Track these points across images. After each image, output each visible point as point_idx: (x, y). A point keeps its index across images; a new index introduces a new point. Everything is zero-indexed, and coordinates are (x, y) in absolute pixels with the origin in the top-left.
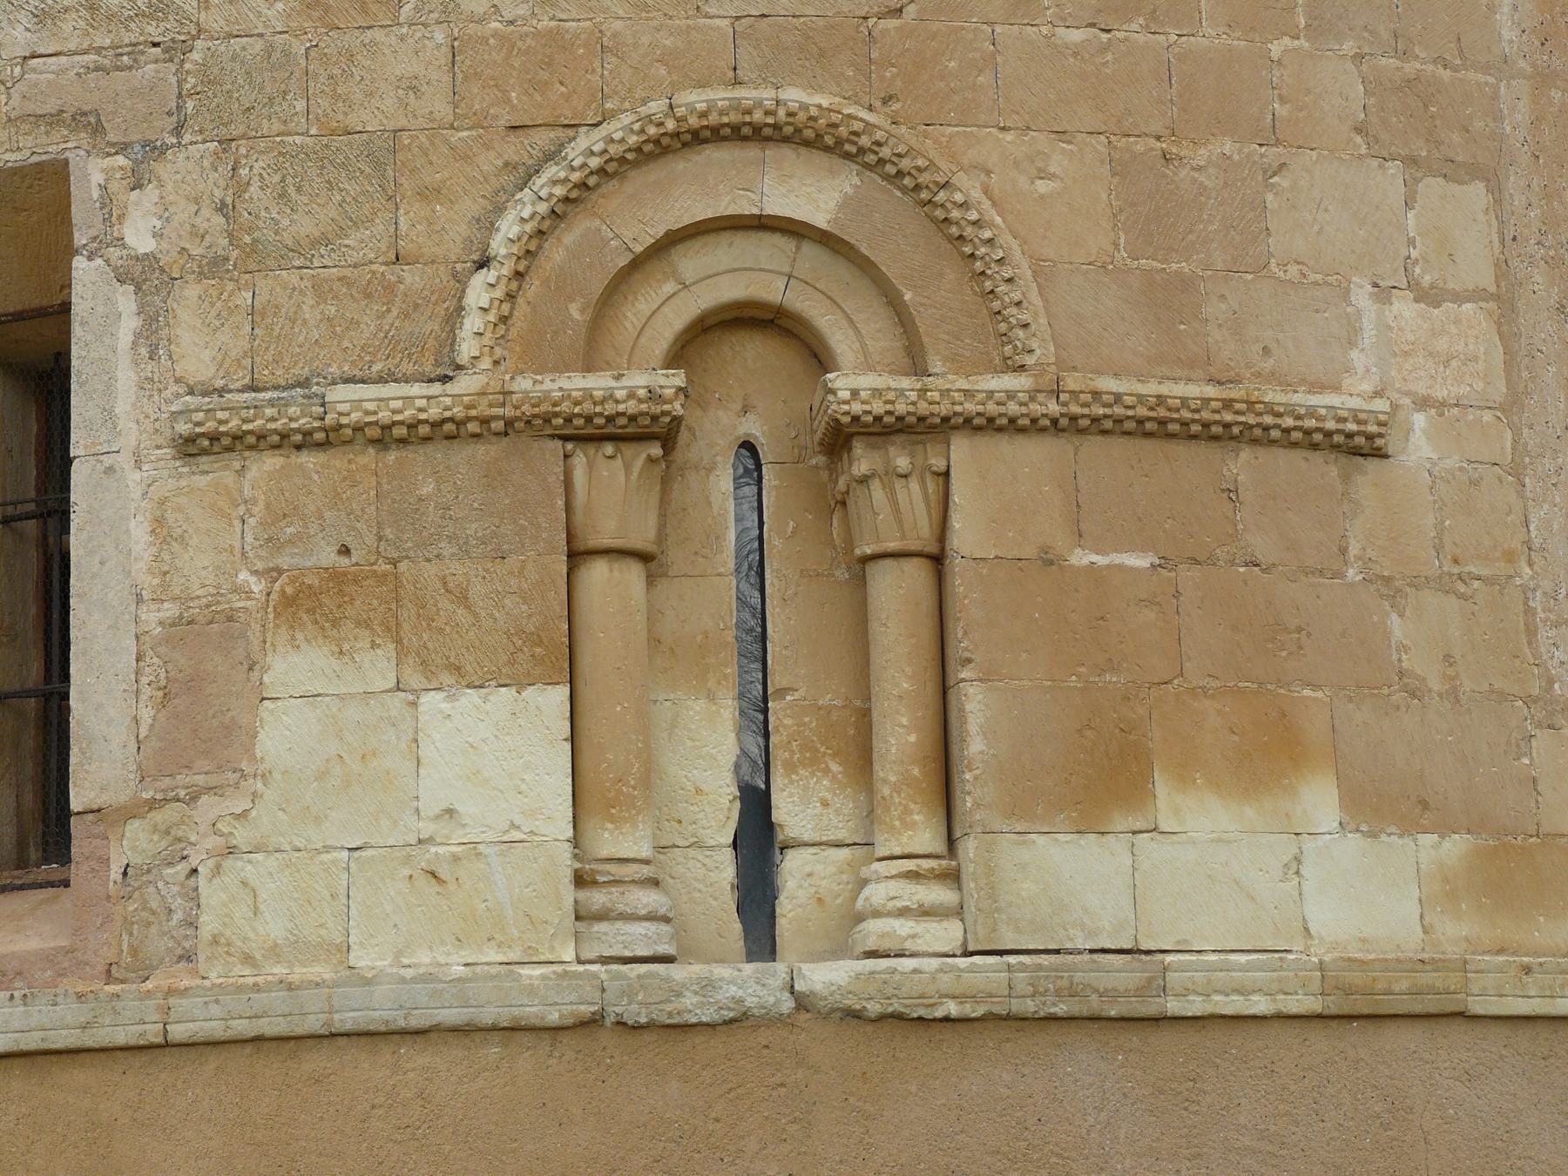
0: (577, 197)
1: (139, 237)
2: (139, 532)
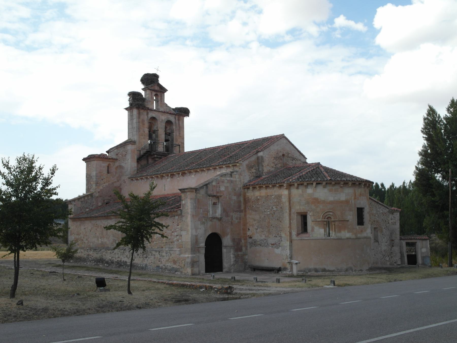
0: (324, 214)
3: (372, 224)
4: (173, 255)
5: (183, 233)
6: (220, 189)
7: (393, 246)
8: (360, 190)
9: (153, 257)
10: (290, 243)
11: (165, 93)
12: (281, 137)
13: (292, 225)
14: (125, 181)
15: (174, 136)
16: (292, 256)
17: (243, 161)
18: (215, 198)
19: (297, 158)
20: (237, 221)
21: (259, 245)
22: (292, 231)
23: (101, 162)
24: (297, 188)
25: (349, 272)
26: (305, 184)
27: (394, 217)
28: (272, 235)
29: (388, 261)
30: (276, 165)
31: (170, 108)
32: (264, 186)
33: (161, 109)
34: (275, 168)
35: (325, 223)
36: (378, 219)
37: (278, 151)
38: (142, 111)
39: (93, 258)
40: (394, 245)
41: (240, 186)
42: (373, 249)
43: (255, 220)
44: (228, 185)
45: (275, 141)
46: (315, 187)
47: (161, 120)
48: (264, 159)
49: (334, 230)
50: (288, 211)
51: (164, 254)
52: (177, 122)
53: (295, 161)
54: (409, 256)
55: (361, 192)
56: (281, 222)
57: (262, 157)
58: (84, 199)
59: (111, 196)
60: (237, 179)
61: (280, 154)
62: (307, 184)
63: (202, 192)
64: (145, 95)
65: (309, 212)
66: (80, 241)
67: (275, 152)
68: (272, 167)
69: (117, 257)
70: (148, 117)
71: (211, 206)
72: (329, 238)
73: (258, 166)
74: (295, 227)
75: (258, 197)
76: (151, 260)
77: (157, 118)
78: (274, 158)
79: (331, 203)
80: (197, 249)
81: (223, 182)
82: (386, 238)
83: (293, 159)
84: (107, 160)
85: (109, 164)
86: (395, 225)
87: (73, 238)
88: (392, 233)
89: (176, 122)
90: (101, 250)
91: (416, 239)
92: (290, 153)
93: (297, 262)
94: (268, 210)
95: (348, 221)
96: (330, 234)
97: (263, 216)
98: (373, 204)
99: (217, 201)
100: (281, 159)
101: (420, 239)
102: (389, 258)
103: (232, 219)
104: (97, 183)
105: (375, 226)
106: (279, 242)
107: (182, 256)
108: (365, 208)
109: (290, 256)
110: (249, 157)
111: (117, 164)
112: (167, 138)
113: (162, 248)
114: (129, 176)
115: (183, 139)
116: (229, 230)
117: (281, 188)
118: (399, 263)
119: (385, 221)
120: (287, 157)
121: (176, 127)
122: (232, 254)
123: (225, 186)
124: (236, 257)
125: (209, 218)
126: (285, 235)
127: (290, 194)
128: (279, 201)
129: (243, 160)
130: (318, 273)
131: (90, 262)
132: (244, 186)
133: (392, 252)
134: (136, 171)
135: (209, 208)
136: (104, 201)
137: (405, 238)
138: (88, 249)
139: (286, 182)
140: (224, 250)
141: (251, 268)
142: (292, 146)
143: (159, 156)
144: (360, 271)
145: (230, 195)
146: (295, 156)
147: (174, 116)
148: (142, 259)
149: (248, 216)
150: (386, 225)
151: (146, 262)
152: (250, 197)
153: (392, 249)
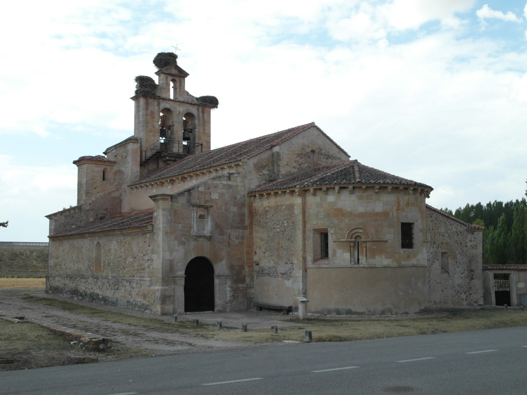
0: (351, 231)
1: (331, 232)
2: (331, 246)
3: (438, 248)
4: (143, 287)
5: (155, 256)
6: (211, 197)
7: (472, 279)
8: (406, 197)
9: (123, 289)
10: (303, 272)
11: (186, 78)
12: (310, 127)
13: (307, 247)
14: (126, 190)
15: (197, 133)
16: (306, 291)
17: (248, 159)
18: (202, 208)
19: (334, 156)
20: (237, 241)
21: (267, 275)
22: (307, 256)
23: (94, 165)
24: (314, 194)
25: (386, 316)
26: (324, 188)
27: (474, 238)
28: (283, 261)
29: (464, 299)
30: (300, 165)
31: (193, 97)
32: (272, 193)
33: (181, 99)
34: (298, 168)
35: (352, 244)
36: (448, 240)
37: (305, 145)
38: (151, 101)
39: (68, 288)
40: (474, 277)
41: (243, 192)
43: (262, 240)
44: (224, 191)
45: (300, 132)
46: (339, 193)
47: (178, 113)
48: (281, 157)
49: (364, 255)
50: (301, 227)
51: (134, 285)
52: (201, 115)
53: (332, 159)
54: (498, 294)
55: (408, 200)
56: (292, 242)
57: (278, 153)
58: (70, 212)
59: (107, 209)
60: (239, 183)
61: (307, 150)
62: (328, 189)
63: (182, 200)
64: (159, 81)
65: (329, 229)
66: (59, 266)
67: (299, 147)
68: (294, 167)
69: (90, 287)
70: (159, 108)
71: (195, 219)
72: (357, 266)
73: (273, 166)
74: (311, 250)
75: (267, 208)
76: (122, 293)
77: (172, 110)
78: (298, 155)
79: (362, 215)
80: (171, 279)
81: (216, 187)
82: (461, 267)
83: (329, 157)
84: (95, 163)
85: (105, 169)
86: (476, 249)
87: (53, 262)
88: (471, 260)
89: (199, 115)
90: (76, 278)
91: (509, 269)
92: (323, 148)
93: (305, 299)
94: (278, 226)
95: (386, 242)
96: (360, 260)
97: (271, 235)
98: (441, 219)
99: (206, 213)
100: (309, 157)
101: (515, 270)
102: (465, 295)
103: (230, 238)
104: (88, 193)
105: (444, 251)
106: (290, 271)
107: (152, 288)
108: (416, 224)
109: (303, 291)
110: (259, 154)
111: (115, 168)
112: (187, 136)
113: (134, 276)
114: (128, 184)
115: (209, 136)
116: (224, 254)
117: (293, 195)
118: (481, 302)
119: (461, 243)
120: (319, 154)
121: (199, 122)
122: (229, 286)
123: (219, 193)
124: (235, 291)
125: (192, 236)
126: (297, 261)
127: (304, 204)
128: (291, 213)
129: (249, 158)
130: (341, 316)
131: (66, 294)
132: (249, 193)
133: (470, 287)
134: (139, 177)
135: (192, 223)
136: (97, 215)
137: (492, 268)
138: (64, 277)
139: (298, 186)
140: (217, 281)
141: (257, 306)
142: (327, 139)
143: (172, 159)
144: (405, 314)
145: (227, 205)
146: (331, 153)
147: (197, 107)
148: (113, 291)
149: (255, 234)
150: (461, 249)
151: (116, 296)
152: (258, 209)
153: (471, 283)
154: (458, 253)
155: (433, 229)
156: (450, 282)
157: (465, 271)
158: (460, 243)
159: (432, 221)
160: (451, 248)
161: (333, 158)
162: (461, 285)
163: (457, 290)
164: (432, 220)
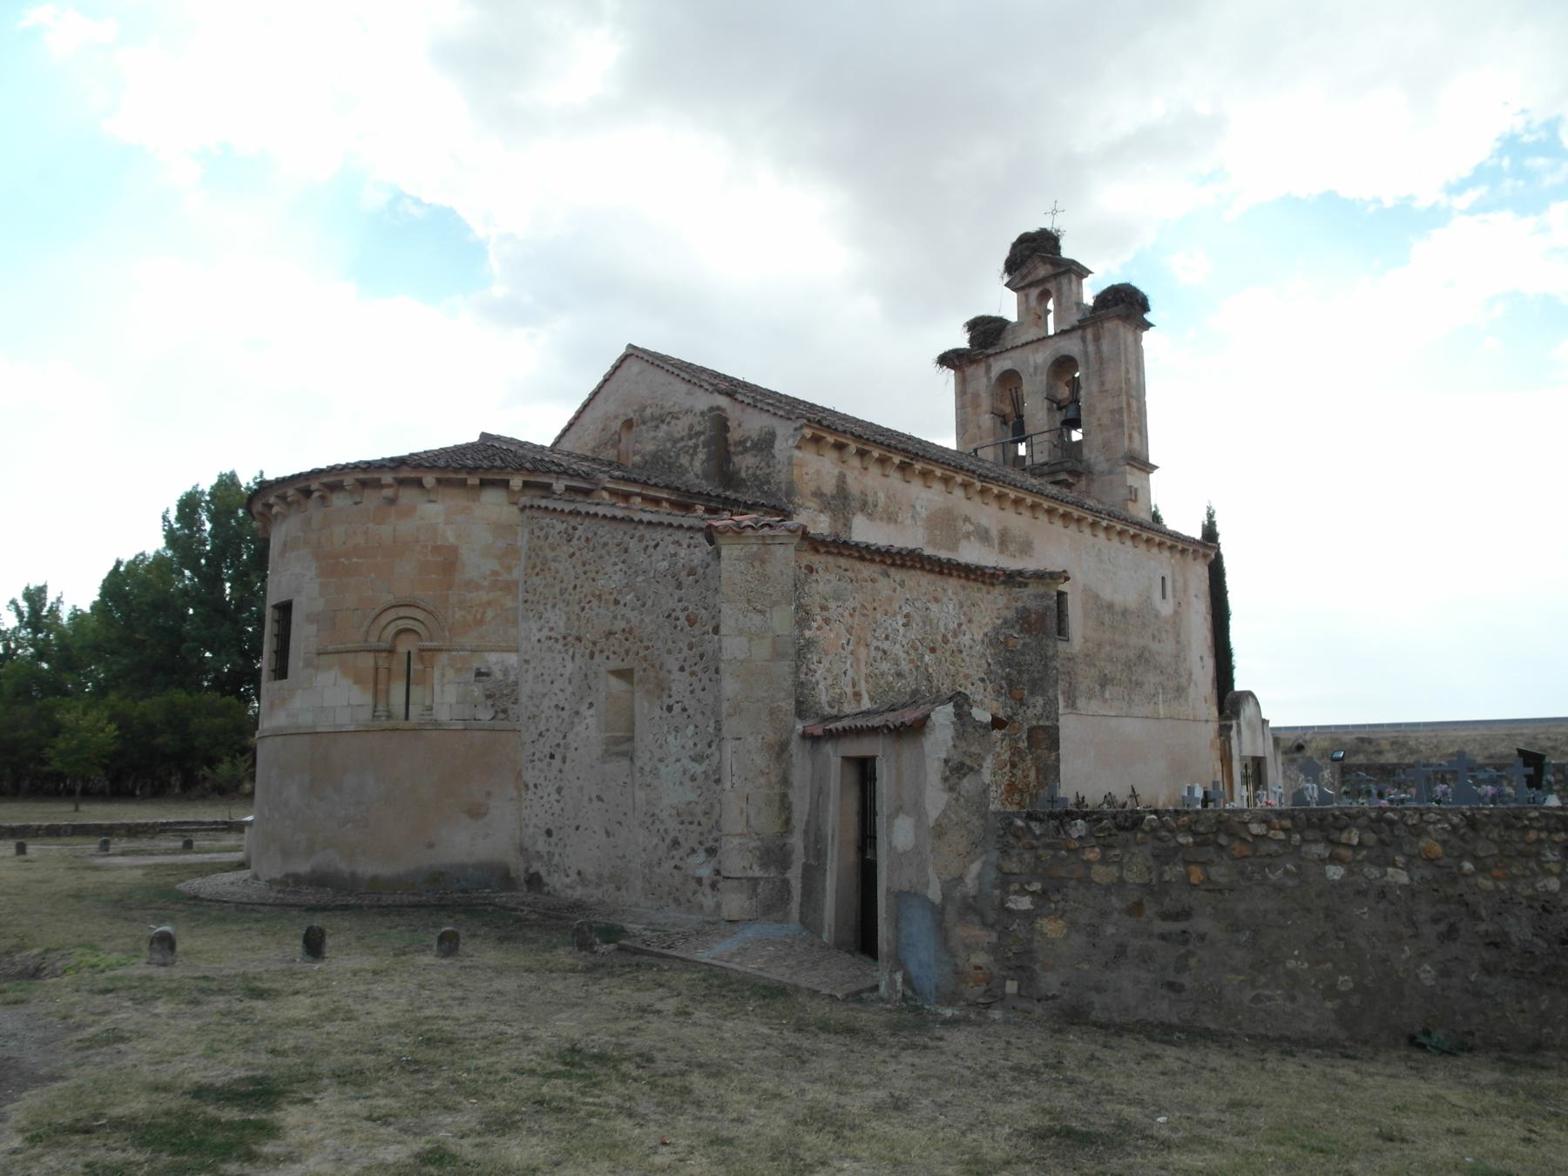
3: (592, 656)
29: (707, 882)
36: (633, 616)
42: (599, 798)
70: (989, 379)
82: (691, 730)
89: (1086, 353)
119: (692, 622)
150: (691, 647)
154: (675, 668)
155: (575, 587)
156: (641, 795)
157: (710, 746)
158: (688, 618)
159: (573, 555)
160: (647, 648)
161: (673, 417)
162: (692, 814)
163: (673, 834)
164: (571, 550)
